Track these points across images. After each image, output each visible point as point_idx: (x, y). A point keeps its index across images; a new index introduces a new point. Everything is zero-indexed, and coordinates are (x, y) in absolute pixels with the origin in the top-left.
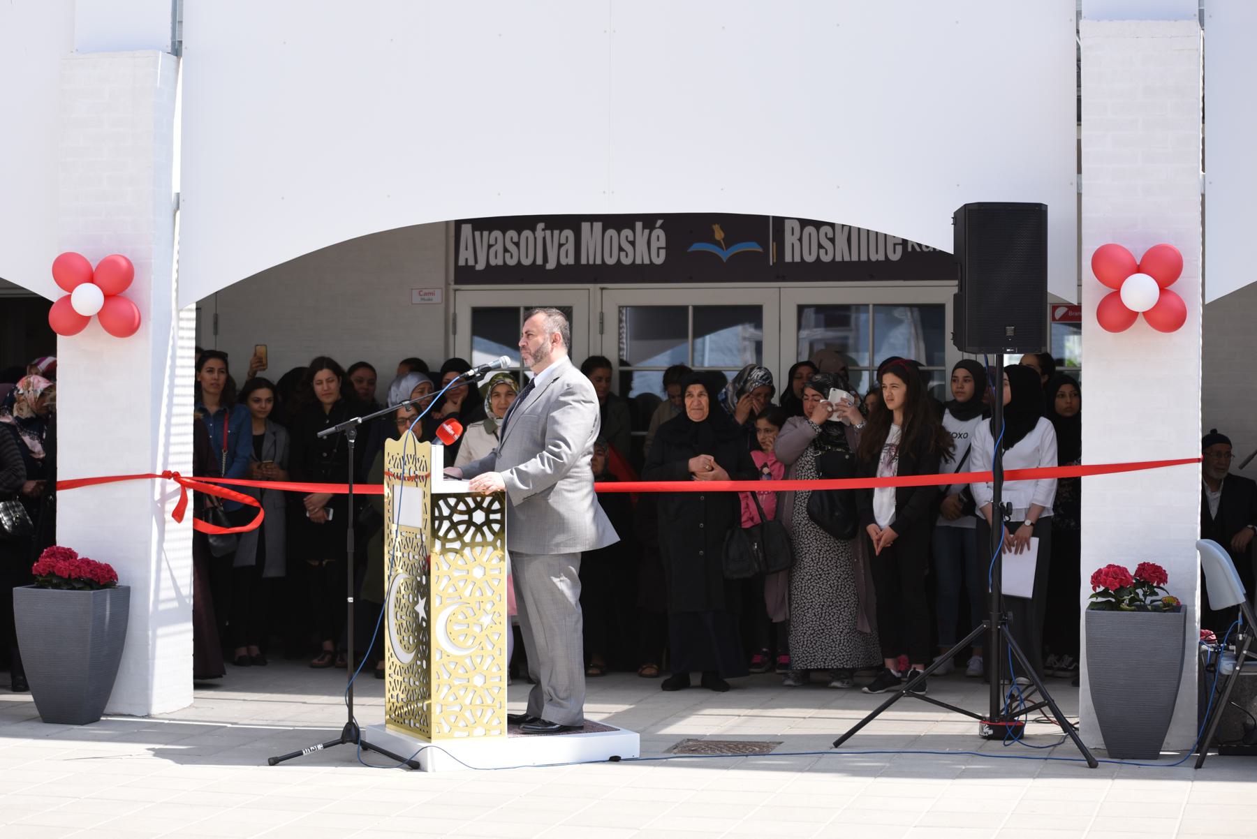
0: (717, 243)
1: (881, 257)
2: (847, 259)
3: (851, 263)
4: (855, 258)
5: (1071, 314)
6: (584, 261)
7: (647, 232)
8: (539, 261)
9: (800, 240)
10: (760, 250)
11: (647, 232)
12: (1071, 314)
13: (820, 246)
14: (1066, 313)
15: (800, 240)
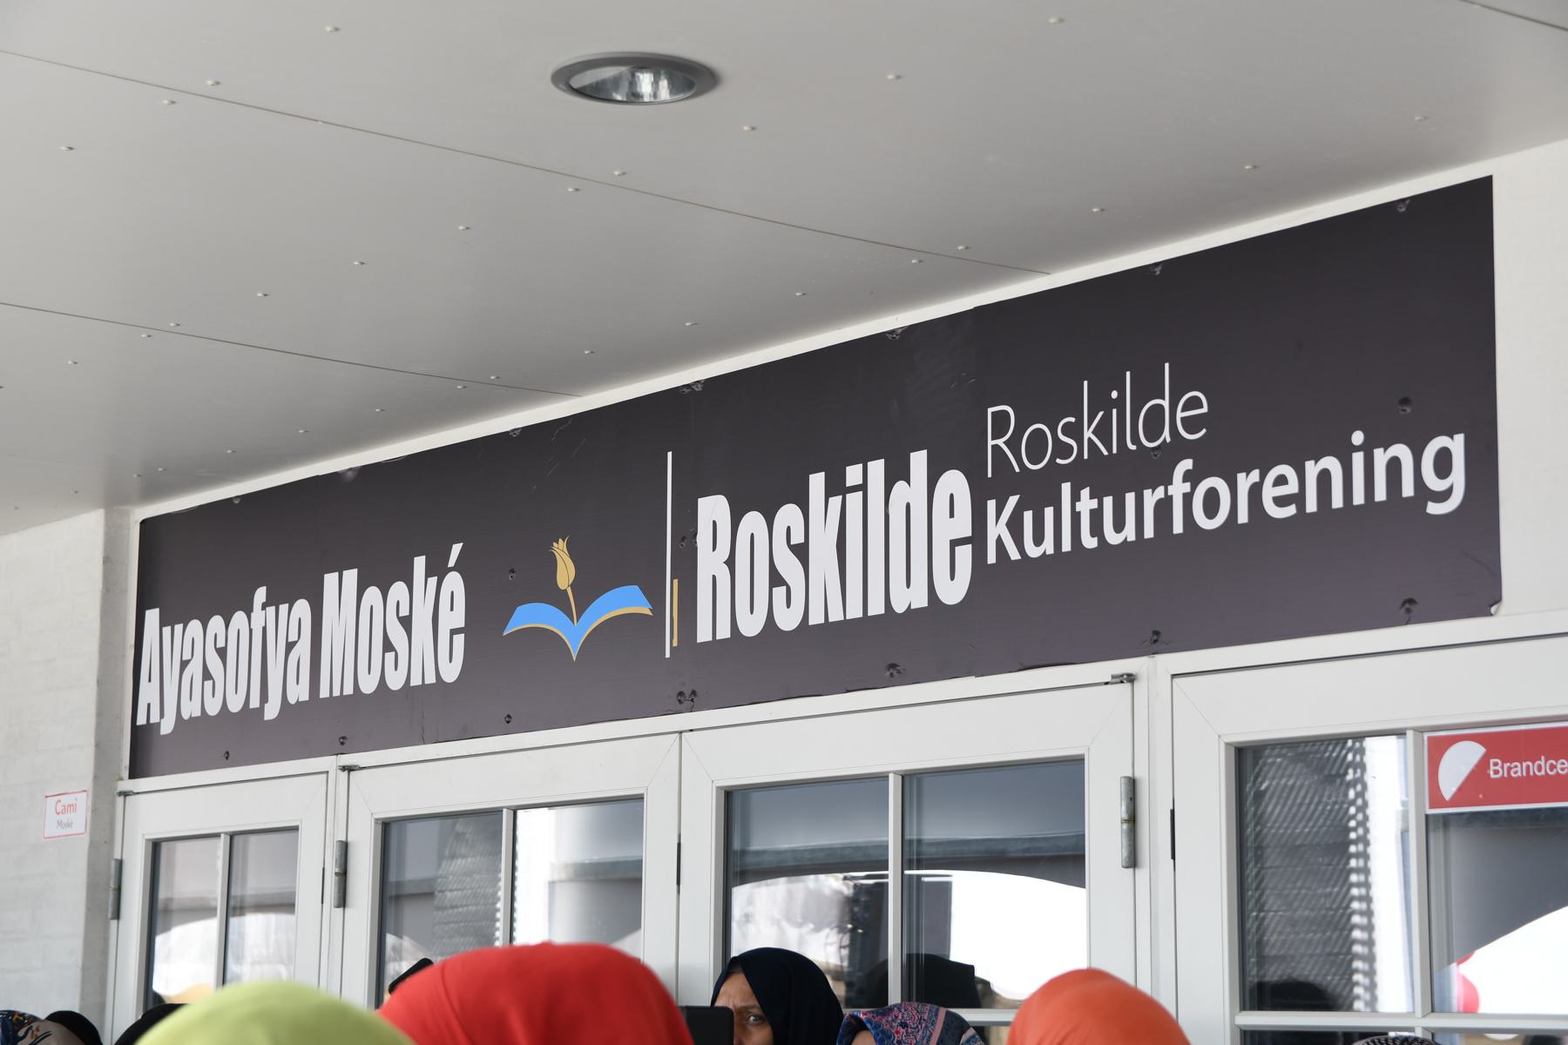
0: (557, 599)
1: (921, 601)
2: (836, 616)
3: (846, 624)
4: (855, 612)
5: (1497, 770)
6: (324, 693)
7: (433, 581)
8: (255, 703)
9: (731, 562)
10: (645, 609)
11: (433, 581)
12: (1497, 770)
13: (776, 579)
14: (1483, 764)
15: (731, 562)
